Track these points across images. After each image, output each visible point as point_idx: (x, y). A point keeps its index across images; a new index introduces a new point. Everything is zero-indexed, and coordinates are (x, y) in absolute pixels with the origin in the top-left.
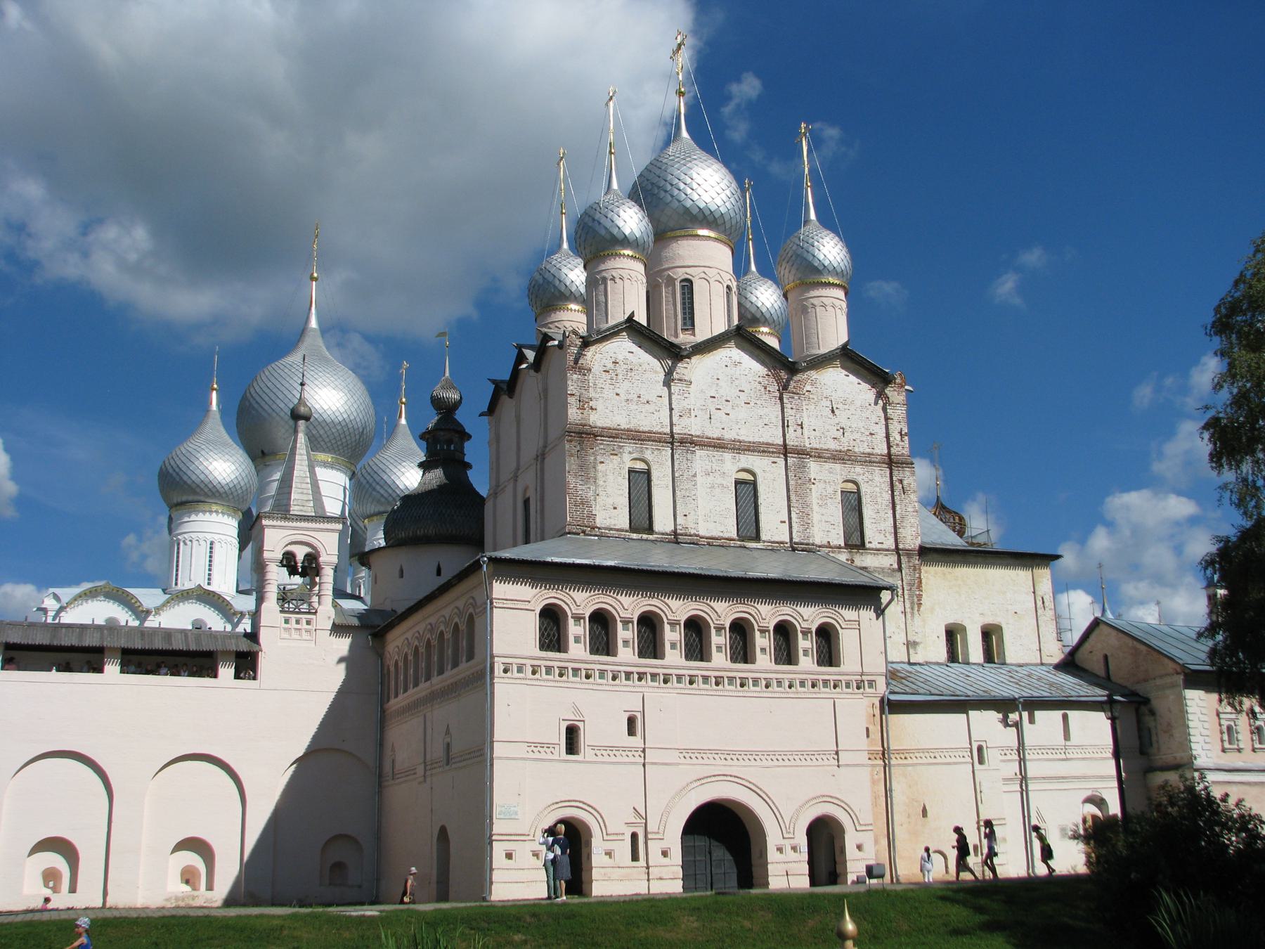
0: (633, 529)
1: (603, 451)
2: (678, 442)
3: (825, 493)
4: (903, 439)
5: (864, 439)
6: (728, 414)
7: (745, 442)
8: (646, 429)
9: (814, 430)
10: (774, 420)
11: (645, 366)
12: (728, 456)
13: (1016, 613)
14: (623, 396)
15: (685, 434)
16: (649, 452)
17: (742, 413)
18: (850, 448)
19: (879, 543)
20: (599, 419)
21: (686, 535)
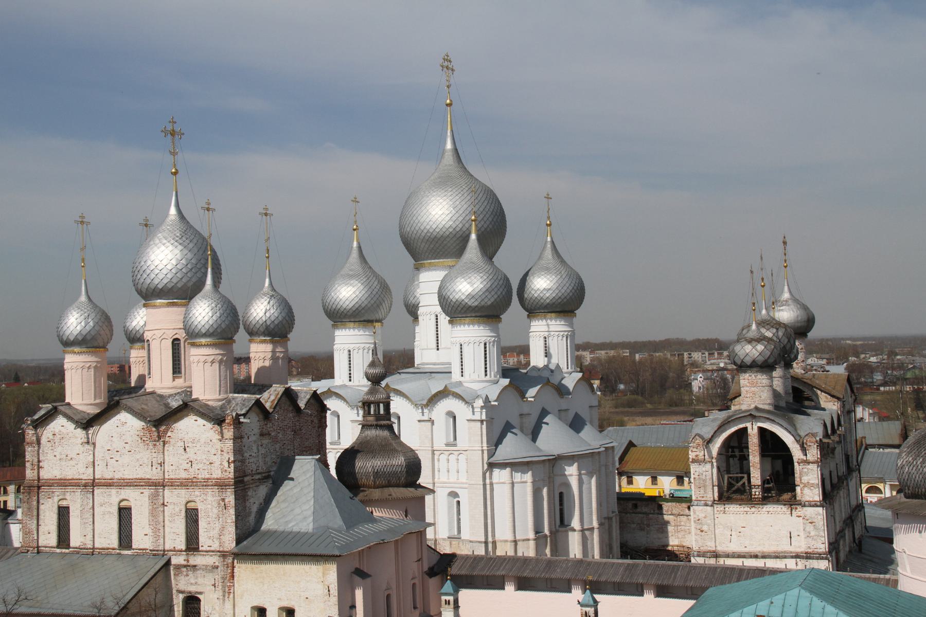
0: (58, 547)
1: (43, 497)
2: (83, 486)
3: (174, 512)
4: (230, 466)
5: (205, 468)
6: (117, 461)
7: (127, 479)
8: (70, 477)
9: (172, 465)
10: (146, 461)
11: (70, 435)
12: (113, 491)
13: (307, 598)
14: (58, 457)
15: (88, 480)
16: (68, 494)
17: (126, 459)
18: (195, 476)
19: (208, 546)
20: (45, 474)
21: (84, 549)
